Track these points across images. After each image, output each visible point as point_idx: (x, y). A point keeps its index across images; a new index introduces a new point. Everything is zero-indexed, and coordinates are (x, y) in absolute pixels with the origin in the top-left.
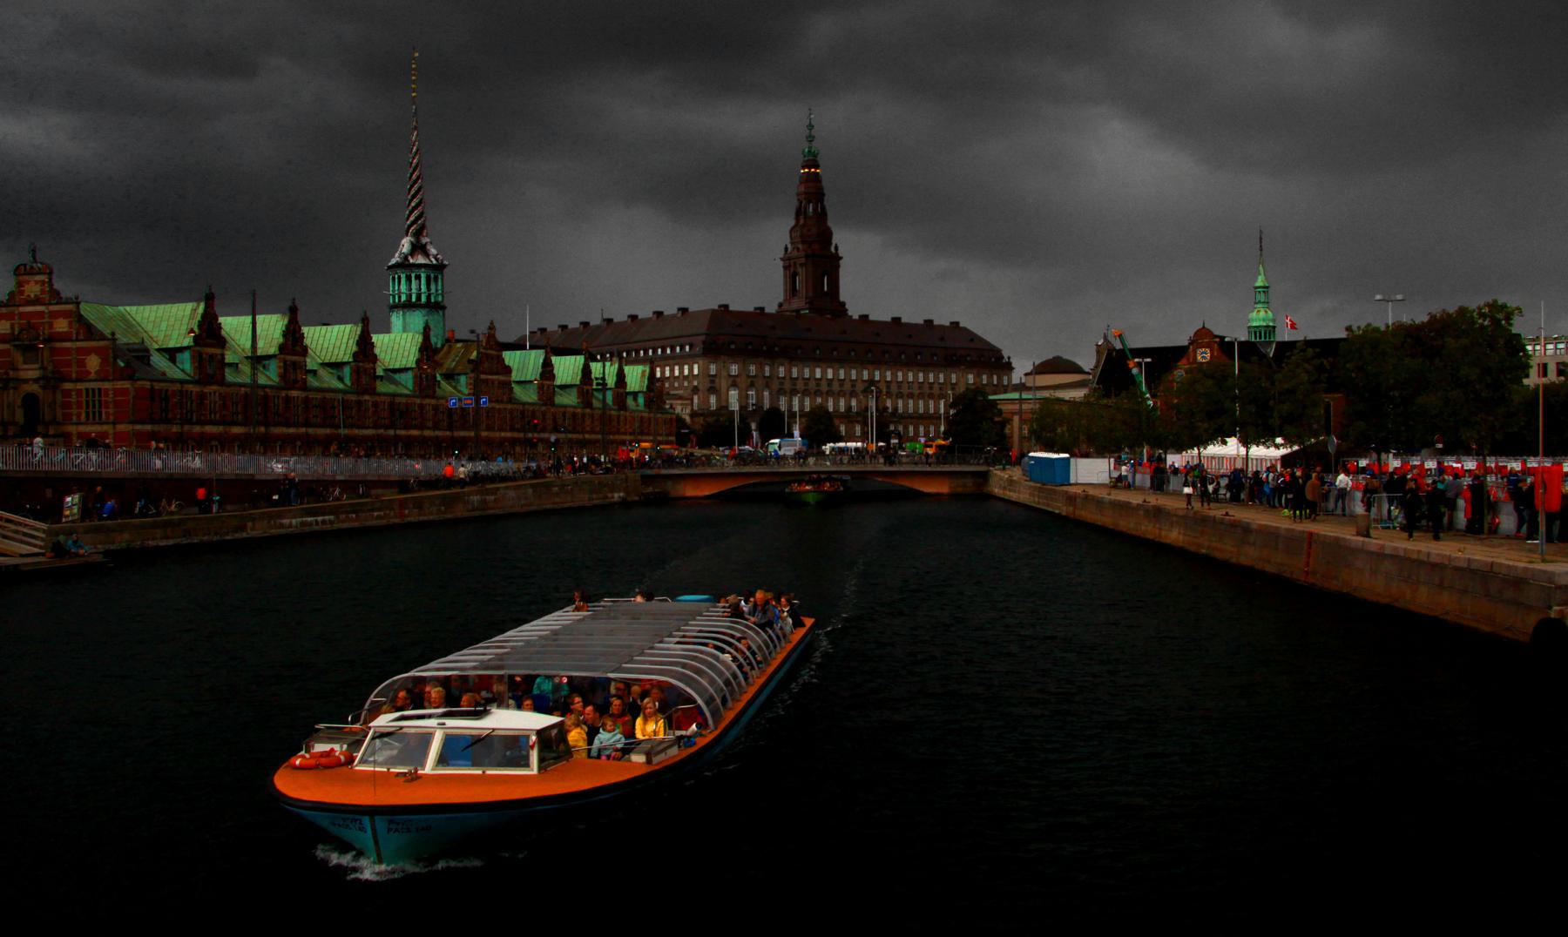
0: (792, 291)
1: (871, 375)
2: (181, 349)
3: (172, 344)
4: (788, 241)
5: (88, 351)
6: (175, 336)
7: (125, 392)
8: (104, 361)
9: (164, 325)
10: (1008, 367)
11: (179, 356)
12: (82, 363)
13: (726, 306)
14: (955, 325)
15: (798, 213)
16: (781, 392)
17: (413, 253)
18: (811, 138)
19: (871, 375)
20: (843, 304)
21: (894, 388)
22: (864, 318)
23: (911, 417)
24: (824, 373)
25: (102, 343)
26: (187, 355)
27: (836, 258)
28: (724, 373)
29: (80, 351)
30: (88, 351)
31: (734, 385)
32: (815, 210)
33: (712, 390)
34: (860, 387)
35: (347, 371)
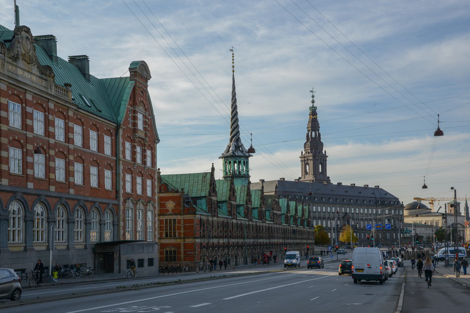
2: (200, 198)
3: (194, 195)
5: (168, 199)
7: (192, 221)
8: (178, 205)
19: (346, 210)
20: (329, 178)
21: (355, 216)
22: (339, 184)
23: (362, 230)
25: (176, 195)
26: (204, 201)
30: (168, 199)
34: (341, 215)
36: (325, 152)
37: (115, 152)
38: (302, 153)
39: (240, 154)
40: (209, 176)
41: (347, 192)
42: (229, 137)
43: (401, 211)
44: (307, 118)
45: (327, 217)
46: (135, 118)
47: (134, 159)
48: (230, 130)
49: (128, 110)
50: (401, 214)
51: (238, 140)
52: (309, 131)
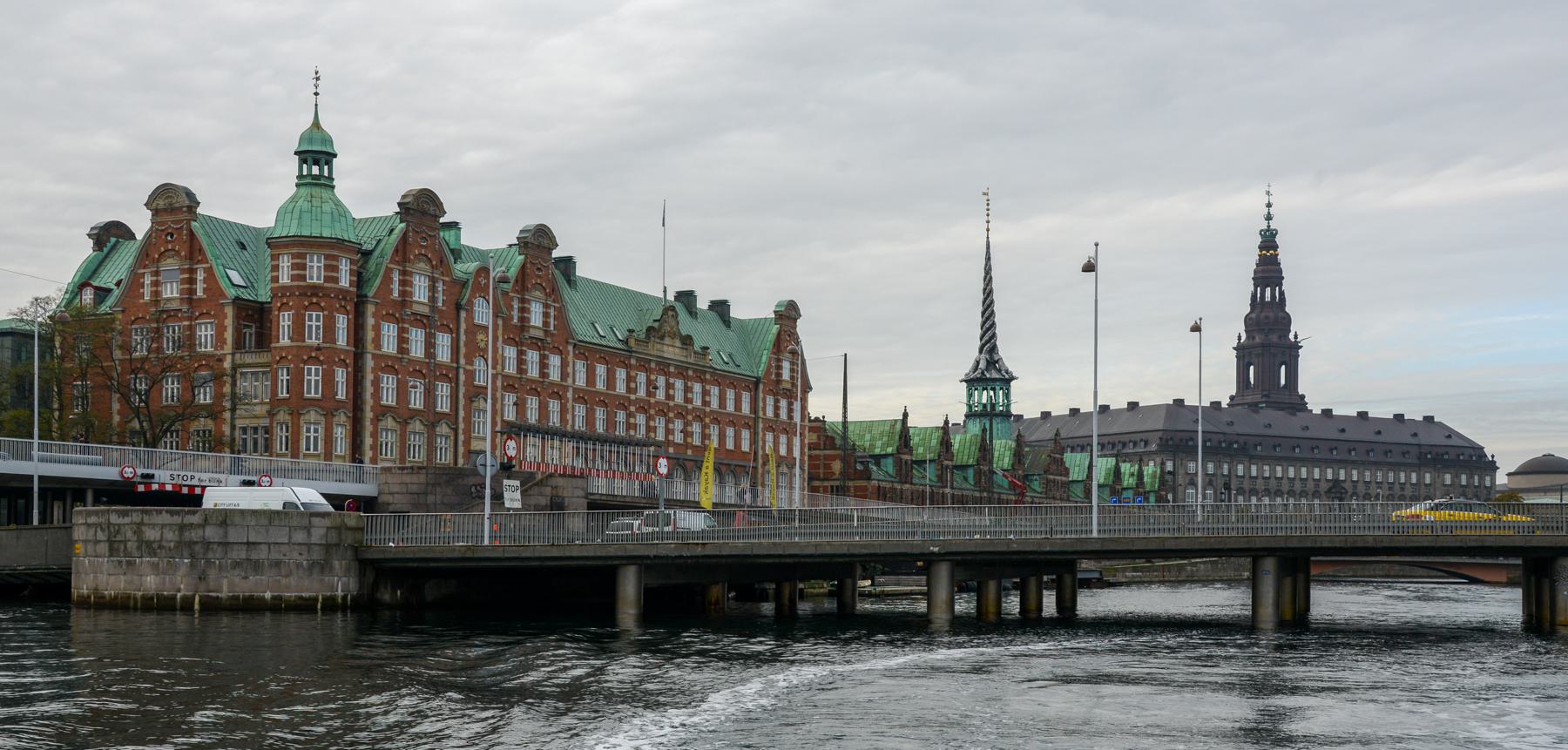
1: (1336, 474)
2: (886, 456)
3: (877, 451)
5: (834, 458)
6: (879, 443)
9: (868, 437)
10: (1492, 467)
11: (883, 461)
12: (828, 467)
15: (1254, 296)
17: (987, 369)
18: (1269, 218)
19: (1336, 474)
20: (1303, 397)
21: (1361, 489)
22: (1327, 413)
24: (1285, 471)
26: (890, 461)
27: (1295, 347)
29: (827, 457)
34: (1324, 487)
35: (971, 472)
37: (754, 409)
39: (997, 376)
40: (899, 426)
41: (1343, 431)
42: (979, 344)
43: (1488, 478)
46: (779, 367)
47: (777, 415)
48: (979, 332)
49: (770, 359)
50: (1488, 484)
51: (993, 349)
52: (1256, 286)
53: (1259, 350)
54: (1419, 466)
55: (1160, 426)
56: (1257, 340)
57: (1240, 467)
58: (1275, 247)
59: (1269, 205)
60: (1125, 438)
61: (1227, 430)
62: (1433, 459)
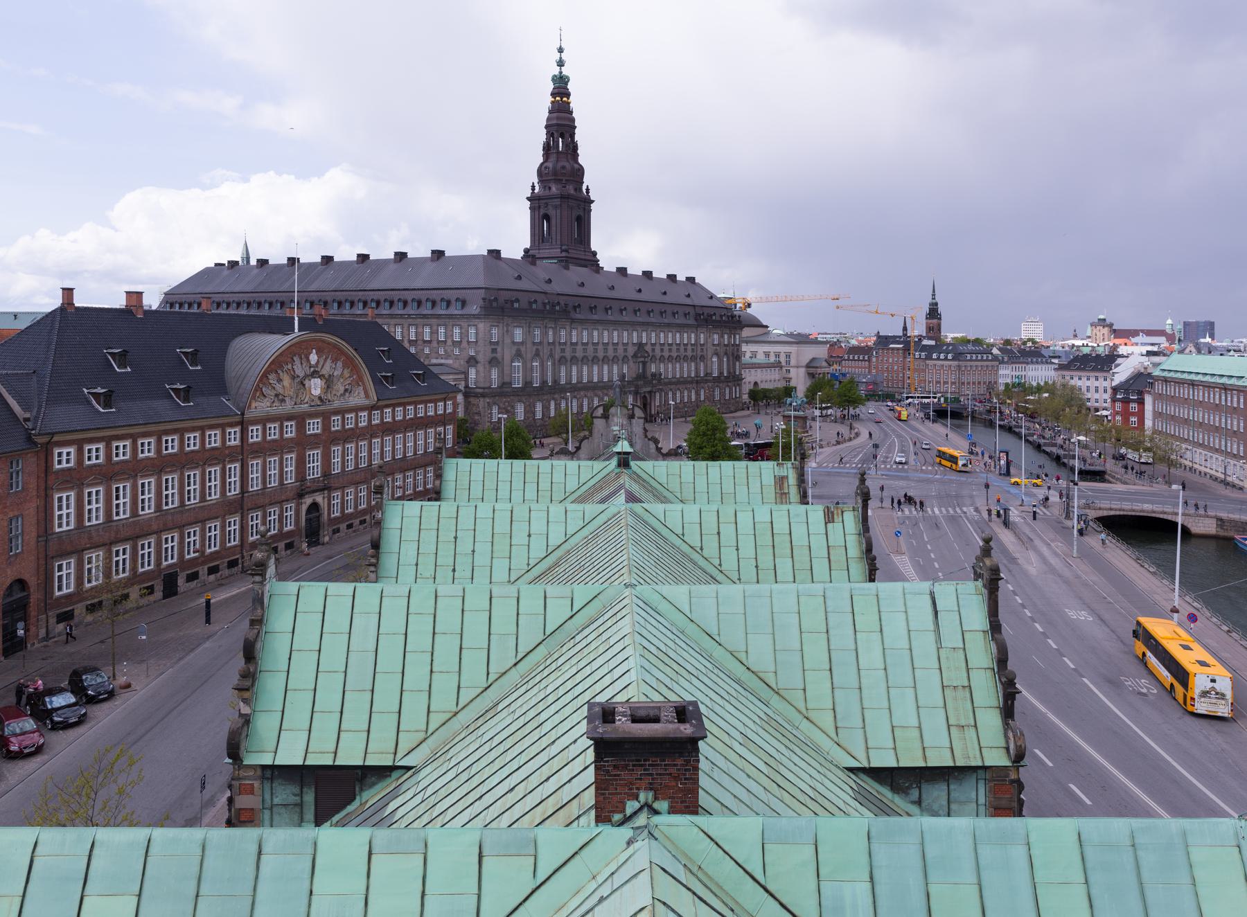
0: (538, 235)
1: (640, 337)
4: (536, 180)
13: (498, 252)
14: (691, 280)
16: (562, 360)
18: (561, 63)
19: (640, 337)
20: (595, 254)
21: (658, 353)
27: (585, 203)
28: (508, 341)
31: (518, 355)
32: (565, 145)
33: (494, 362)
34: (631, 350)
36: (588, 190)
38: (533, 187)
44: (547, 101)
45: (601, 354)
53: (557, 202)
54: (697, 326)
55: (480, 282)
56: (554, 189)
57: (563, 333)
58: (568, 95)
59: (561, 50)
60: (435, 295)
61: (547, 288)
62: (706, 321)
